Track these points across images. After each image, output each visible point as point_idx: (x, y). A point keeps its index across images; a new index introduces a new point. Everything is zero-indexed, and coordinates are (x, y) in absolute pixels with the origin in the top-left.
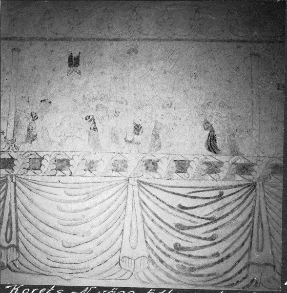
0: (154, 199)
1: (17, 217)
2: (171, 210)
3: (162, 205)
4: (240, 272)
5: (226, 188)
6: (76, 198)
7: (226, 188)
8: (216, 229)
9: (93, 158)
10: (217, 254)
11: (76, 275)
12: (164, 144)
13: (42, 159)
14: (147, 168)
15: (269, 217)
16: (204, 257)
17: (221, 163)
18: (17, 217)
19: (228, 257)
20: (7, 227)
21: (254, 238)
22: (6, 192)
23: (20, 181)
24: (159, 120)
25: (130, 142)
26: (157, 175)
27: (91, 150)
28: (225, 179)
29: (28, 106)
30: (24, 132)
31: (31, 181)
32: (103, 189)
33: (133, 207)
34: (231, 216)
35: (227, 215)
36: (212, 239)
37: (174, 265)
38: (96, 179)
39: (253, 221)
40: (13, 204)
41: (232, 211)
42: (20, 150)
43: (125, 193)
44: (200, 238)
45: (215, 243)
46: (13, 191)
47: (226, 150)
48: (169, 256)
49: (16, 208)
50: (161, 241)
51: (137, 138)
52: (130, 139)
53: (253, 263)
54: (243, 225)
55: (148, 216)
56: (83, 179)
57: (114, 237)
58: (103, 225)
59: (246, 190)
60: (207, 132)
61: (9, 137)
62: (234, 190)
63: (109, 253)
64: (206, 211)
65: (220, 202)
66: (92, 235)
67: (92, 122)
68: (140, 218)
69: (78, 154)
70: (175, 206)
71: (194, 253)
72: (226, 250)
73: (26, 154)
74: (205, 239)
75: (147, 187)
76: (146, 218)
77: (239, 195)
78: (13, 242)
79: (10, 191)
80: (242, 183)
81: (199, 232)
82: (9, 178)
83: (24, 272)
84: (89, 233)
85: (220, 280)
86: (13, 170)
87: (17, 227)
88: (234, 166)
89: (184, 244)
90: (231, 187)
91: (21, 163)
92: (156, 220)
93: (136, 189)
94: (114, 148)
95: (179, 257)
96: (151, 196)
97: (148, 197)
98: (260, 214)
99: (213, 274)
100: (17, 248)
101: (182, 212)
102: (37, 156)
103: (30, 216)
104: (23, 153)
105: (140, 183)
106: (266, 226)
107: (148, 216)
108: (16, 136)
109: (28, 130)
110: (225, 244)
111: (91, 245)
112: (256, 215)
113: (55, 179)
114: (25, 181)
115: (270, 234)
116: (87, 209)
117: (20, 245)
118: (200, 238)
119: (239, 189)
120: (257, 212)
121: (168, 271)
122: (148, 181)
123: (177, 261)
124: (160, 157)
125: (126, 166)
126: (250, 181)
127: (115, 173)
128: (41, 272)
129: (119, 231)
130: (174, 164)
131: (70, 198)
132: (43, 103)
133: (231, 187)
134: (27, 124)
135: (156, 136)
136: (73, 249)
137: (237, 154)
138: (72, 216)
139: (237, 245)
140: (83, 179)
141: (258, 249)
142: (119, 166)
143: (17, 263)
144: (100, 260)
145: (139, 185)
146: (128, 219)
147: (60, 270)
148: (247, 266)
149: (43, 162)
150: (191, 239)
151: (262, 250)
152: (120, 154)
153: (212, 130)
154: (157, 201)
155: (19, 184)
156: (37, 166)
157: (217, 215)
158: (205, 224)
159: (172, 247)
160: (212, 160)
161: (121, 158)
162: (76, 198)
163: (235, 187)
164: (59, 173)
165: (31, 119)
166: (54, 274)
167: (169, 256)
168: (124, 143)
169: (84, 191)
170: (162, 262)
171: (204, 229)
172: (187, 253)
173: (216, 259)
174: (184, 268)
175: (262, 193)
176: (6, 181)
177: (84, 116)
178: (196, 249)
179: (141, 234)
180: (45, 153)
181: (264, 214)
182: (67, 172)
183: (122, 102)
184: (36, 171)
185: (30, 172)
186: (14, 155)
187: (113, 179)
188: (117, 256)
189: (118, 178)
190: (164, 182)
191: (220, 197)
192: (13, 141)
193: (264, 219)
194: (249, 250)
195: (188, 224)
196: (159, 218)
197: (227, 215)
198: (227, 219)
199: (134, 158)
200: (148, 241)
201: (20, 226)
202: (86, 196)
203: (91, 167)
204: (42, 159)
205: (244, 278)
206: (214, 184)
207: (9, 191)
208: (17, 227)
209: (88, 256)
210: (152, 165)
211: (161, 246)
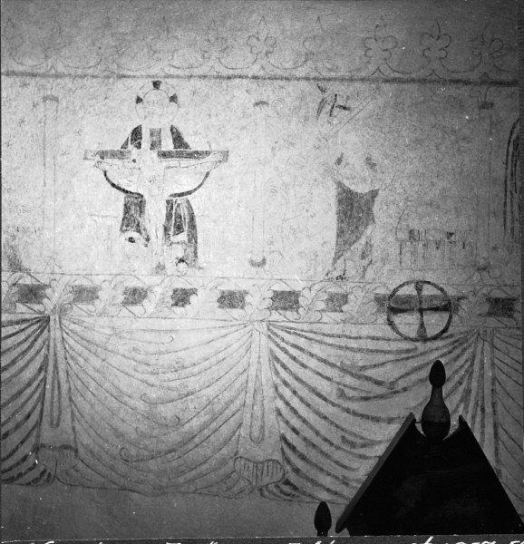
15: (70, 372)
21: (47, 404)
39: (45, 379)
53: (43, 446)
59: (35, 327)
77: (22, 336)
80: (27, 316)
88: (15, 289)
112: (51, 368)
115: (70, 400)
119: (26, 325)
126: (40, 313)
137: (20, 270)
141: (51, 424)
151: (58, 425)
163: (17, 323)
175: (58, 333)
181: (62, 367)
193: (62, 375)
194: (39, 423)
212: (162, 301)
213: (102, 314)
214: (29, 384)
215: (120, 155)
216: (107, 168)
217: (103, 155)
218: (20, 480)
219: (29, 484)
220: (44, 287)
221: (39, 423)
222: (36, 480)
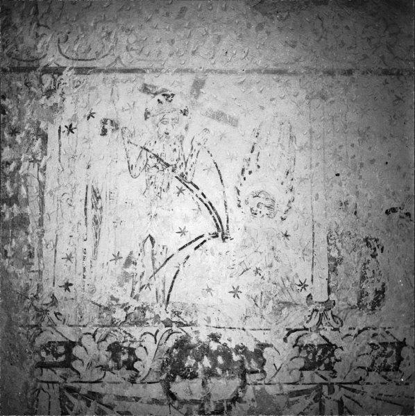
61: (320, 295)
86: (335, 372)
104: (356, 332)
184: (391, 374)
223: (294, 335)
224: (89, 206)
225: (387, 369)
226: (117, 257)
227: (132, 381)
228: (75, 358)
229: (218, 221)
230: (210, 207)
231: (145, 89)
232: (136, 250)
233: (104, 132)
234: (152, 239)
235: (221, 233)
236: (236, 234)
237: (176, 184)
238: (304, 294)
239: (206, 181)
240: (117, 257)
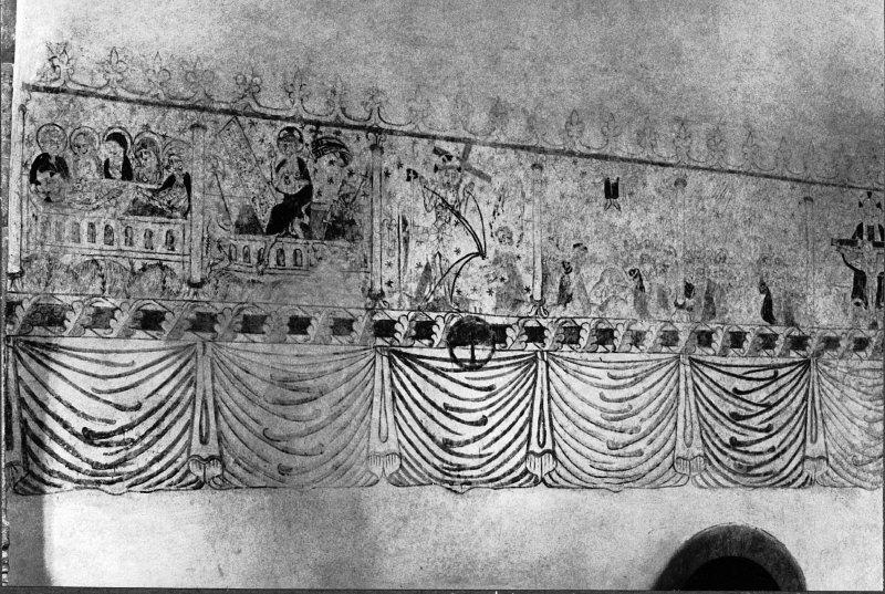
0: (708, 381)
1: (550, 410)
2: (726, 396)
3: (717, 389)
4: (795, 468)
5: (780, 366)
6: (622, 382)
7: (780, 366)
8: (771, 418)
9: (638, 327)
10: (773, 449)
11: (626, 485)
12: (718, 310)
13: (580, 328)
14: (700, 343)
16: (760, 453)
17: (776, 336)
18: (550, 410)
19: (784, 451)
20: (539, 424)
22: (536, 376)
23: (554, 360)
24: (712, 279)
25: (681, 307)
26: (711, 352)
27: (637, 317)
28: (780, 356)
29: (558, 252)
30: (556, 289)
31: (567, 359)
32: (653, 370)
33: (687, 393)
34: (786, 401)
35: (782, 400)
36: (767, 430)
37: (731, 464)
38: (644, 357)
40: (546, 393)
41: (787, 395)
42: (551, 316)
43: (676, 374)
44: (756, 430)
45: (771, 436)
46: (545, 374)
47: (780, 320)
48: (725, 454)
49: (550, 397)
50: (717, 435)
51: (690, 302)
52: (680, 302)
53: (808, 457)
54: (797, 412)
55: (703, 404)
56: (628, 357)
57: (665, 434)
58: (655, 417)
59: (800, 369)
60: (763, 296)
61: (537, 297)
62: (788, 369)
63: (662, 453)
64: (760, 396)
65: (774, 384)
66: (642, 430)
67: (638, 279)
68: (693, 405)
69: (623, 322)
70: (731, 390)
71: (751, 449)
72: (781, 443)
73: (561, 321)
74: (761, 431)
75: (701, 367)
76: (700, 406)
78: (549, 446)
79: (541, 373)
81: (754, 422)
82: (539, 354)
83: (563, 487)
84: (637, 429)
85: (777, 479)
87: (551, 424)
89: (741, 438)
90: (786, 365)
91: (553, 334)
92: (711, 408)
93: (688, 369)
94: (663, 315)
95: (736, 455)
96: (705, 379)
97: (702, 380)
98: (813, 398)
99: (771, 472)
100: (553, 453)
101: (737, 398)
102: (573, 325)
103: (566, 409)
105: (691, 359)
106: (819, 412)
107: (703, 404)
108: (545, 296)
109: (561, 287)
110: (781, 436)
111: (641, 445)
112: (810, 399)
113: (596, 356)
114: (560, 360)
116: (634, 397)
117: (557, 449)
118: (756, 430)
120: (810, 395)
121: (726, 472)
122: (701, 358)
123: (735, 459)
124: (714, 326)
125: (677, 339)
127: (664, 349)
128: (584, 484)
129: (671, 426)
130: (729, 336)
131: (614, 383)
132: (577, 249)
133: (786, 365)
134: (558, 279)
135: (709, 299)
136: (621, 452)
138: (615, 407)
139: (792, 437)
140: (628, 357)
141: (812, 441)
142: (669, 339)
143: (554, 475)
144: (651, 463)
145: (691, 364)
146: (681, 409)
147: (607, 480)
148: (804, 459)
149: (582, 333)
150: (748, 432)
152: (671, 323)
153: (768, 294)
154: (712, 385)
155: (552, 363)
156: (574, 339)
157: (772, 400)
158: (761, 413)
159: (728, 442)
160: (768, 331)
161: (671, 328)
162: (622, 382)
164: (601, 348)
165: (563, 271)
166: (601, 486)
167: (725, 454)
168: (674, 309)
169: (630, 372)
170: (718, 461)
171: (761, 418)
172: (742, 449)
173: (771, 455)
174: (740, 467)
176: (535, 360)
177: (628, 269)
178: (752, 443)
179: (697, 427)
180: (584, 320)
181: (817, 398)
182: (610, 347)
183: (671, 253)
185: (566, 347)
186: (544, 323)
187: (662, 356)
188: (670, 457)
189: (666, 354)
190: (718, 360)
191: (775, 378)
192: (542, 302)
194: (804, 441)
195: (744, 412)
196: (715, 407)
197: (782, 400)
198: (782, 405)
199: (683, 326)
200: (705, 437)
201: (554, 421)
202: (633, 379)
203: (637, 339)
204: (580, 328)
205: (800, 476)
206: (768, 361)
207: (539, 371)
208: (551, 424)
209: (638, 459)
210: (705, 339)
211: (717, 442)
212: (876, 348)
213: (841, 358)
214: (797, 412)
215: (852, 243)
216: (843, 251)
217: (842, 242)
218: (795, 485)
219: (799, 487)
220: (807, 337)
221: (804, 441)
222: (803, 484)
223: (522, 321)
224: (401, 230)
225: (572, 343)
226: (419, 266)
227: (431, 346)
228: (396, 331)
229: (479, 246)
230: (475, 236)
231: (436, 151)
232: (430, 260)
233: (409, 179)
234: (440, 256)
235: (481, 253)
236: (490, 254)
237: (454, 218)
238: (529, 295)
239: (474, 221)
240: (419, 266)
